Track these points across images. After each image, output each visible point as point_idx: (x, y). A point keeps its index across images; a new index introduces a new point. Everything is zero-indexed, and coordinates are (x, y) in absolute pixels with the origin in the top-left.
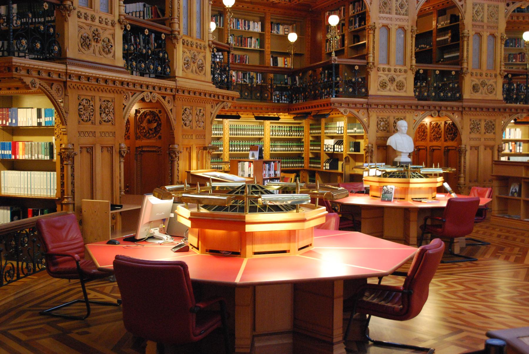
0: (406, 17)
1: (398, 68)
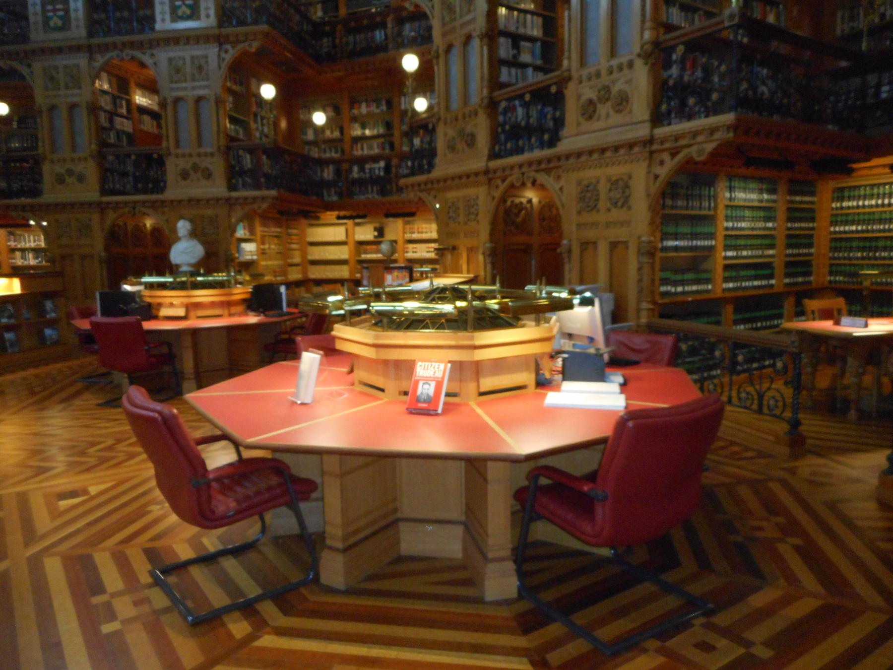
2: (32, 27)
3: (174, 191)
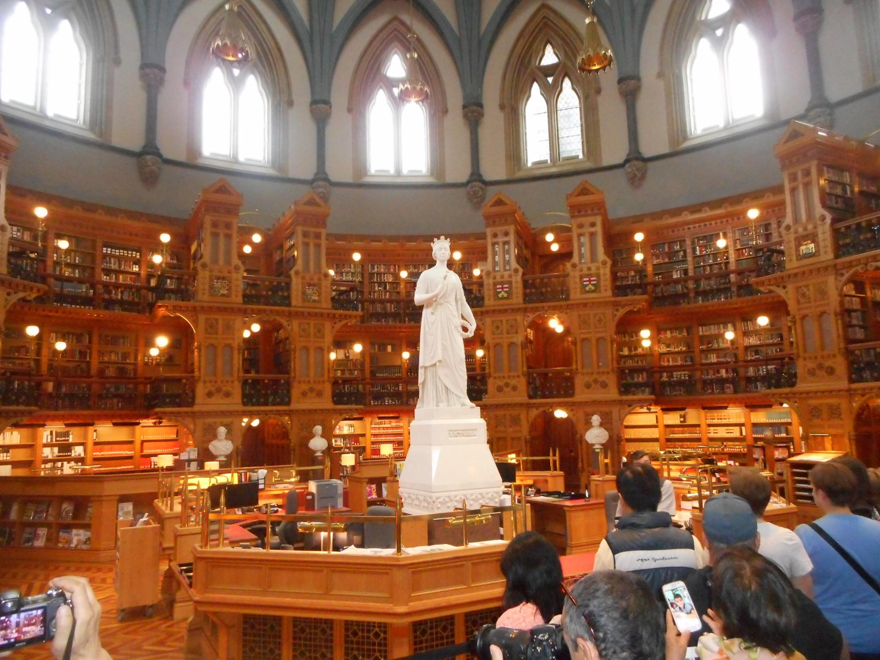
2: (486, 298)
3: (581, 395)
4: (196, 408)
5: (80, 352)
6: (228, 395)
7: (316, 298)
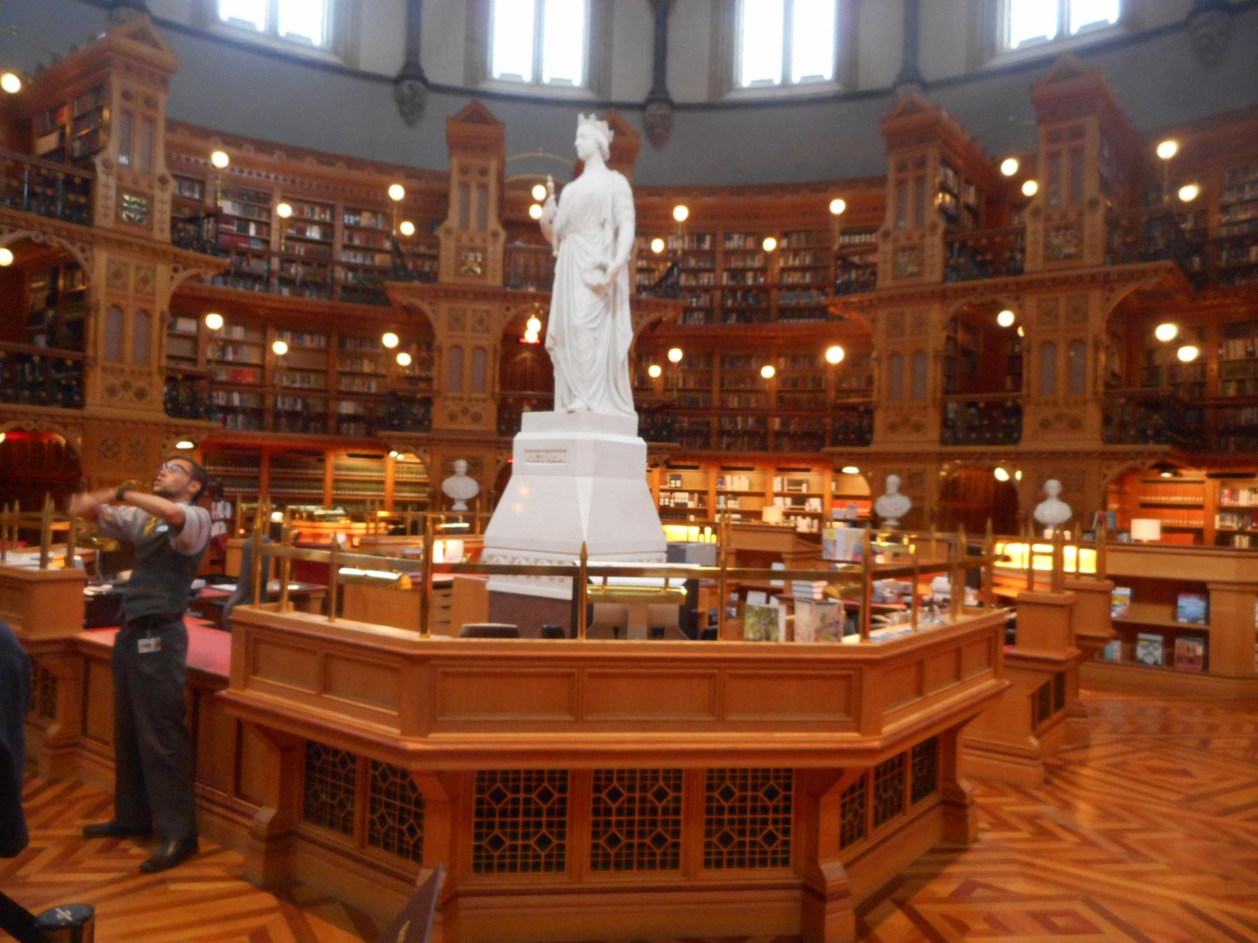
0: (486, 335)
1: (475, 395)
4: (872, 448)
5: (814, 379)
6: (918, 428)
7: (1071, 250)
